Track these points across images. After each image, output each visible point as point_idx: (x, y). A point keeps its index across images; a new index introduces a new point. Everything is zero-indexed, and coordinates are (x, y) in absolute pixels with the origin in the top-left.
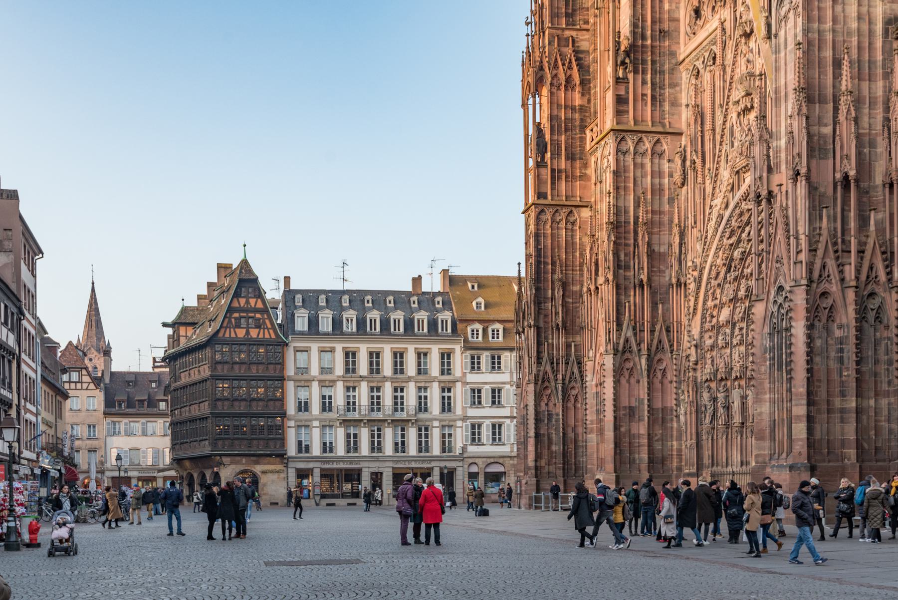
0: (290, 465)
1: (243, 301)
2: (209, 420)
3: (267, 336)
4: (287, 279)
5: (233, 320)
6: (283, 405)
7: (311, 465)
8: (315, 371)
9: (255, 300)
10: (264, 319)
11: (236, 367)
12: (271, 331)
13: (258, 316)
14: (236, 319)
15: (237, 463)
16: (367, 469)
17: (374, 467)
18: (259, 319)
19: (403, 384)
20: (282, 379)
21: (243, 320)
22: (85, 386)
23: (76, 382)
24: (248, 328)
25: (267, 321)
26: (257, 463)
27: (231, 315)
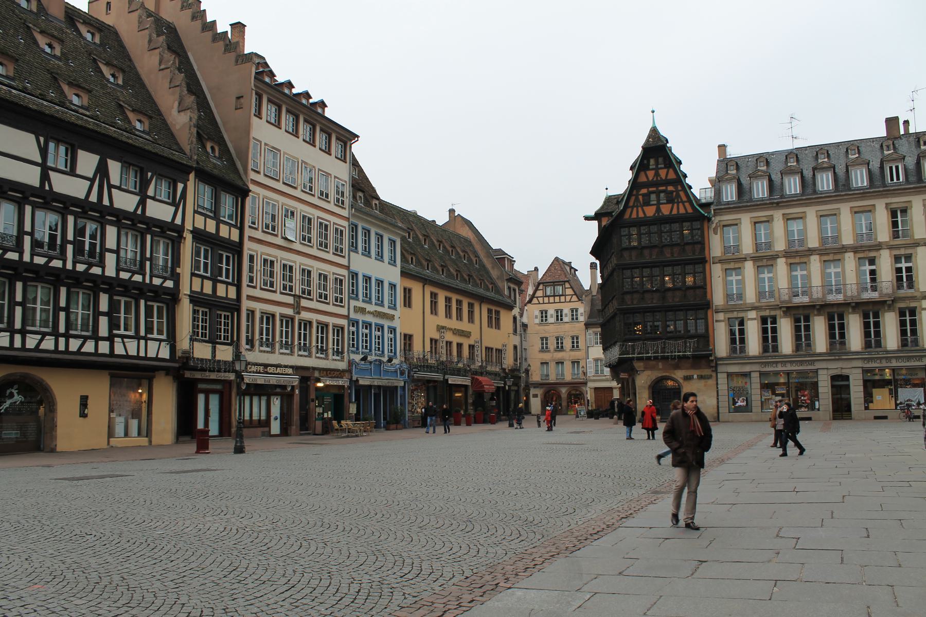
0: (720, 369)
1: (651, 174)
2: (617, 319)
3: (682, 211)
4: (722, 148)
5: (640, 197)
6: (705, 293)
7: (747, 369)
8: (747, 247)
9: (665, 170)
10: (677, 191)
11: (646, 252)
12: (687, 204)
13: (670, 188)
14: (643, 195)
15: (652, 368)
16: (825, 372)
17: (836, 367)
18: (672, 192)
19: (872, 254)
20: (701, 261)
21: (653, 197)
22: (568, 298)
23: (560, 296)
24: (659, 204)
25: (682, 193)
26: (677, 367)
27: (638, 192)
